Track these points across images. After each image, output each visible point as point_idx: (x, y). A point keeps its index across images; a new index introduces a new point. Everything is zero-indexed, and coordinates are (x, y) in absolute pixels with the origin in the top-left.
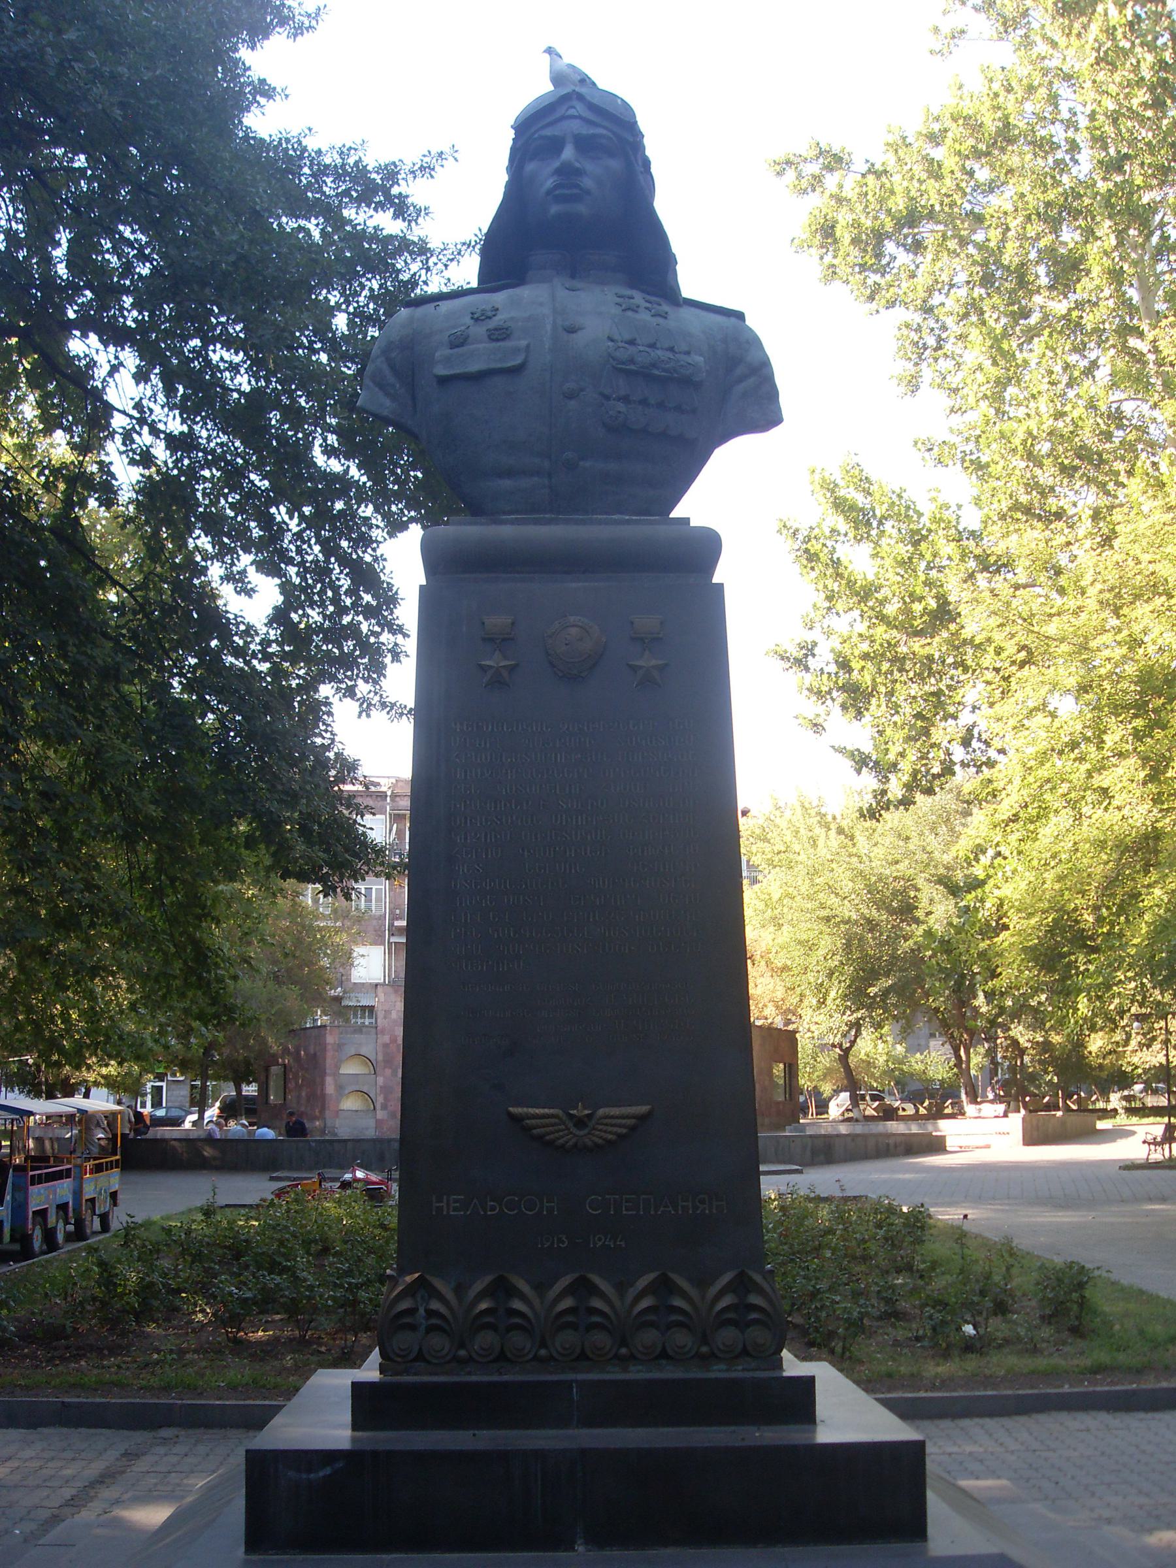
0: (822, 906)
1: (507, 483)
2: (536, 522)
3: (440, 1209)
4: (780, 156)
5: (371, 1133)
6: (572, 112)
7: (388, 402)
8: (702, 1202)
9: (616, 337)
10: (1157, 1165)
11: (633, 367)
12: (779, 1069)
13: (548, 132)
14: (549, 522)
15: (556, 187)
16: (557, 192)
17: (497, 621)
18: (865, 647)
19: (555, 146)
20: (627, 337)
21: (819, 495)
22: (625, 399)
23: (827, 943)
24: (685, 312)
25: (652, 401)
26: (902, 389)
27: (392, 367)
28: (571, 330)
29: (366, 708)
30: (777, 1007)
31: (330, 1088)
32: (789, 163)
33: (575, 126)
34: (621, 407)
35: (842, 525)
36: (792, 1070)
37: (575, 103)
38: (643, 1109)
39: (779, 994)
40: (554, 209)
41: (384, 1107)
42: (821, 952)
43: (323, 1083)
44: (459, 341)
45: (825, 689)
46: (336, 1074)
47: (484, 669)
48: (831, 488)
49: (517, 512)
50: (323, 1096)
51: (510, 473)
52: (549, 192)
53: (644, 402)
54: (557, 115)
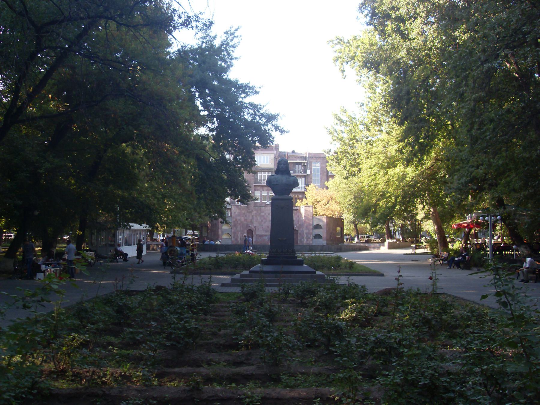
0: (349, 187)
4: (329, 40)
5: (230, 244)
10: (412, 254)
12: (338, 229)
18: (340, 150)
19: (281, 164)
21: (334, 116)
23: (350, 197)
24: (292, 177)
26: (357, 83)
29: (249, 173)
30: (338, 212)
31: (220, 232)
32: (330, 41)
35: (338, 122)
36: (342, 229)
39: (339, 209)
41: (234, 237)
42: (348, 199)
43: (218, 231)
44: (274, 181)
45: (332, 159)
46: (221, 229)
48: (336, 115)
50: (218, 234)
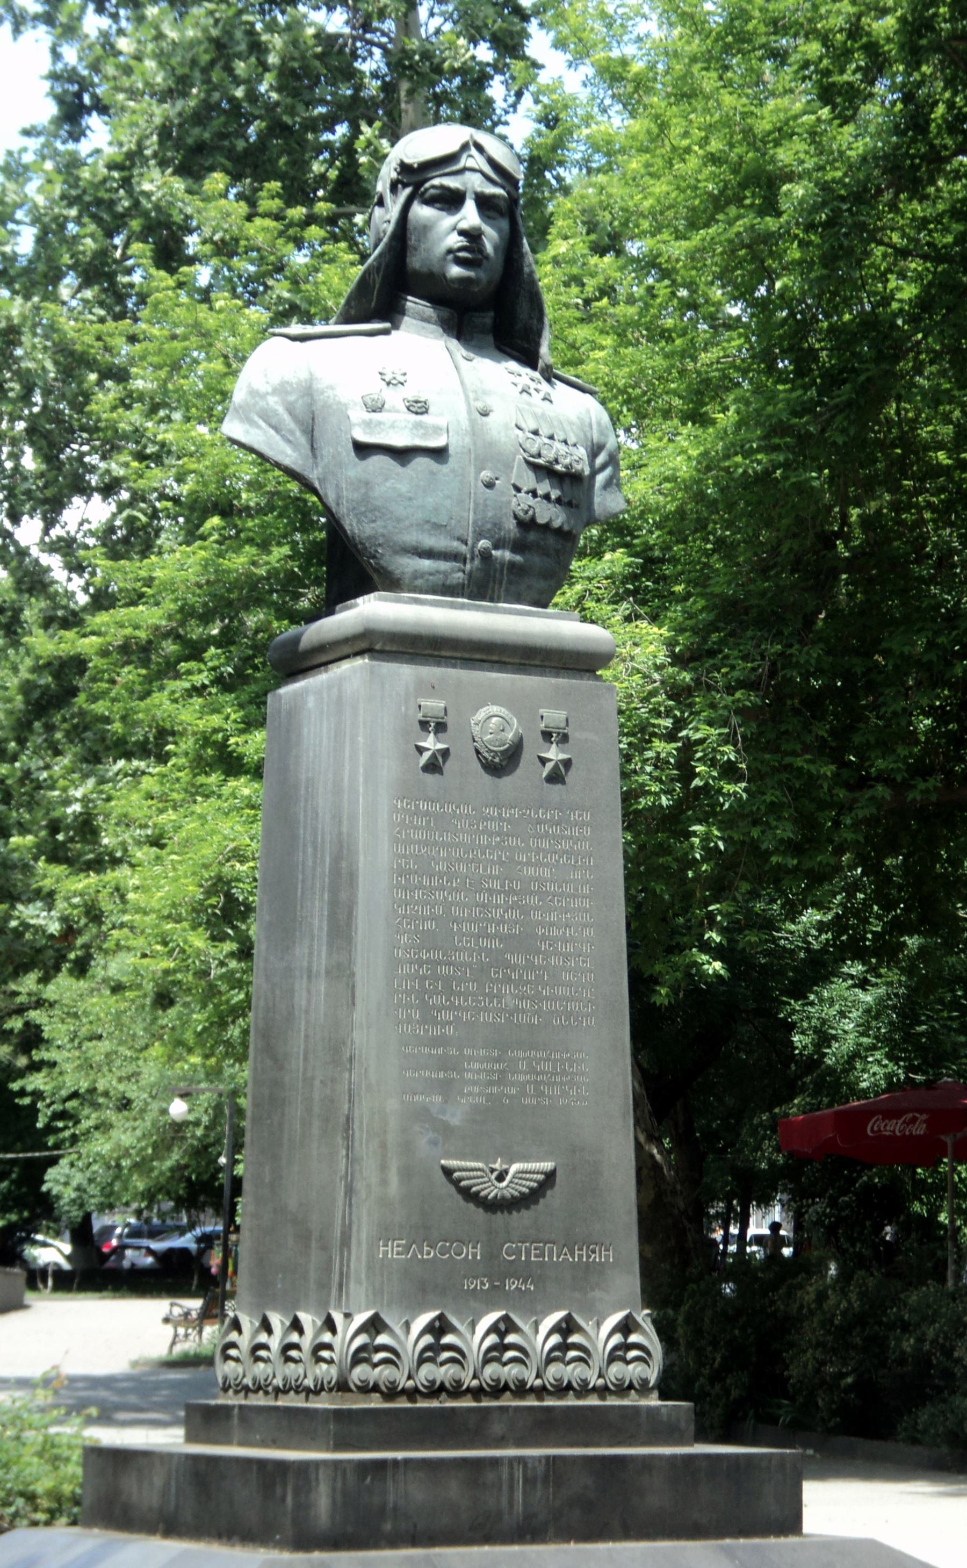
1: (426, 564)
2: (452, 606)
3: (386, 1253)
6: (470, 163)
7: (288, 450)
8: (594, 1252)
9: (523, 425)
11: (541, 461)
13: (452, 183)
14: (462, 607)
15: (461, 249)
16: (461, 254)
17: (433, 705)
20: (533, 426)
22: (534, 493)
25: (540, 492)
27: (290, 411)
28: (485, 414)
33: (475, 183)
34: (530, 500)
37: (473, 151)
38: (548, 1166)
40: (455, 271)
47: (420, 750)
49: (434, 592)
51: (429, 554)
52: (450, 251)
53: (547, 497)
54: (461, 165)
